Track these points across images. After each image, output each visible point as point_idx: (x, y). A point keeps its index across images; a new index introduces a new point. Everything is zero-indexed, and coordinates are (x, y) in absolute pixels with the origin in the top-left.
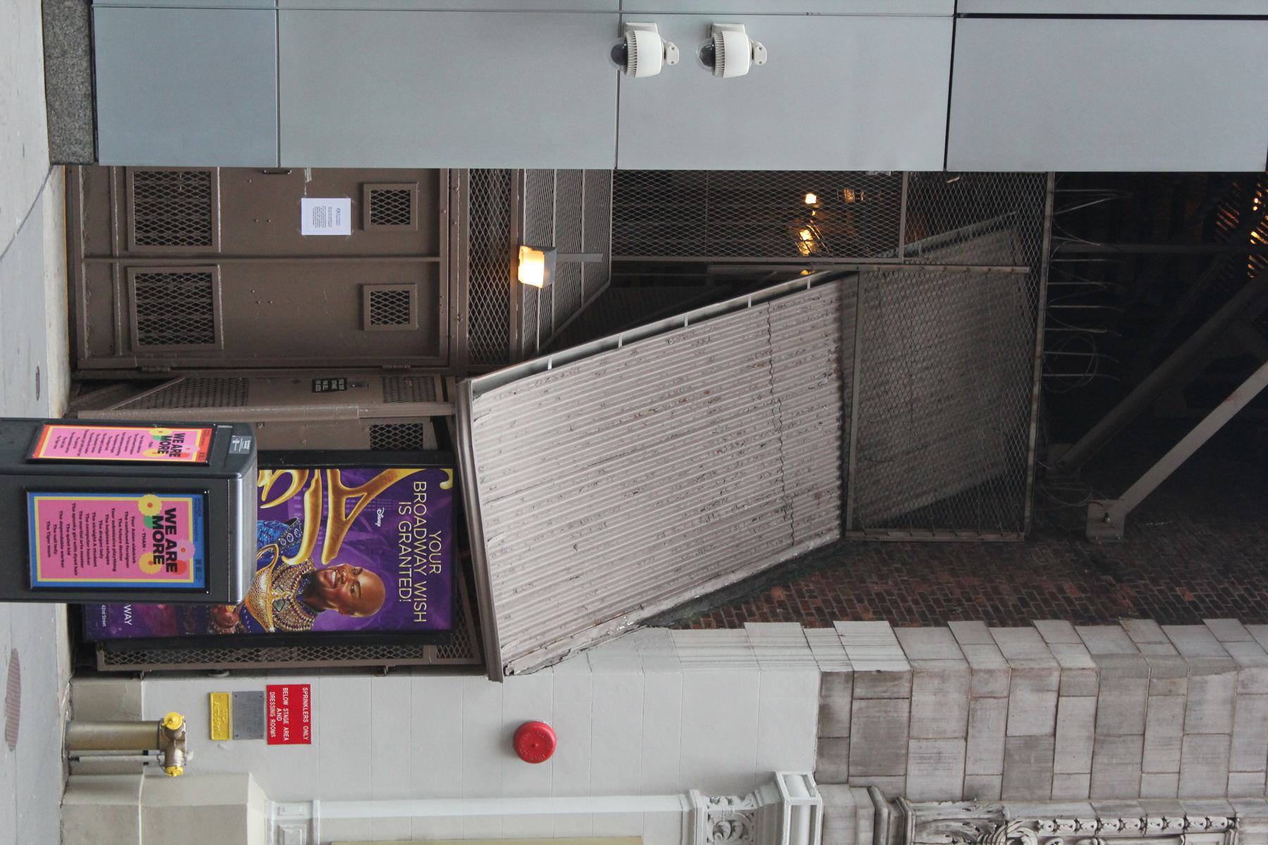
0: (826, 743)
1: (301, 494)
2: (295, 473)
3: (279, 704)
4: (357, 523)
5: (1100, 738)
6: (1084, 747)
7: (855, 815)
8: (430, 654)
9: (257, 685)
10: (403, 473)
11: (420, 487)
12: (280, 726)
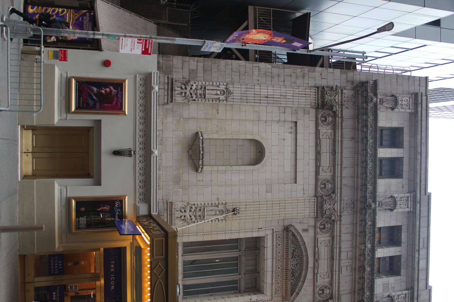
0: (159, 68)
1: (66, 13)
2: (65, 9)
3: (62, 53)
4: (76, 20)
5: (205, 71)
6: (202, 72)
7: (164, 76)
8: (89, 46)
9: (58, 49)
10: (85, 11)
11: (88, 14)
12: (62, 57)
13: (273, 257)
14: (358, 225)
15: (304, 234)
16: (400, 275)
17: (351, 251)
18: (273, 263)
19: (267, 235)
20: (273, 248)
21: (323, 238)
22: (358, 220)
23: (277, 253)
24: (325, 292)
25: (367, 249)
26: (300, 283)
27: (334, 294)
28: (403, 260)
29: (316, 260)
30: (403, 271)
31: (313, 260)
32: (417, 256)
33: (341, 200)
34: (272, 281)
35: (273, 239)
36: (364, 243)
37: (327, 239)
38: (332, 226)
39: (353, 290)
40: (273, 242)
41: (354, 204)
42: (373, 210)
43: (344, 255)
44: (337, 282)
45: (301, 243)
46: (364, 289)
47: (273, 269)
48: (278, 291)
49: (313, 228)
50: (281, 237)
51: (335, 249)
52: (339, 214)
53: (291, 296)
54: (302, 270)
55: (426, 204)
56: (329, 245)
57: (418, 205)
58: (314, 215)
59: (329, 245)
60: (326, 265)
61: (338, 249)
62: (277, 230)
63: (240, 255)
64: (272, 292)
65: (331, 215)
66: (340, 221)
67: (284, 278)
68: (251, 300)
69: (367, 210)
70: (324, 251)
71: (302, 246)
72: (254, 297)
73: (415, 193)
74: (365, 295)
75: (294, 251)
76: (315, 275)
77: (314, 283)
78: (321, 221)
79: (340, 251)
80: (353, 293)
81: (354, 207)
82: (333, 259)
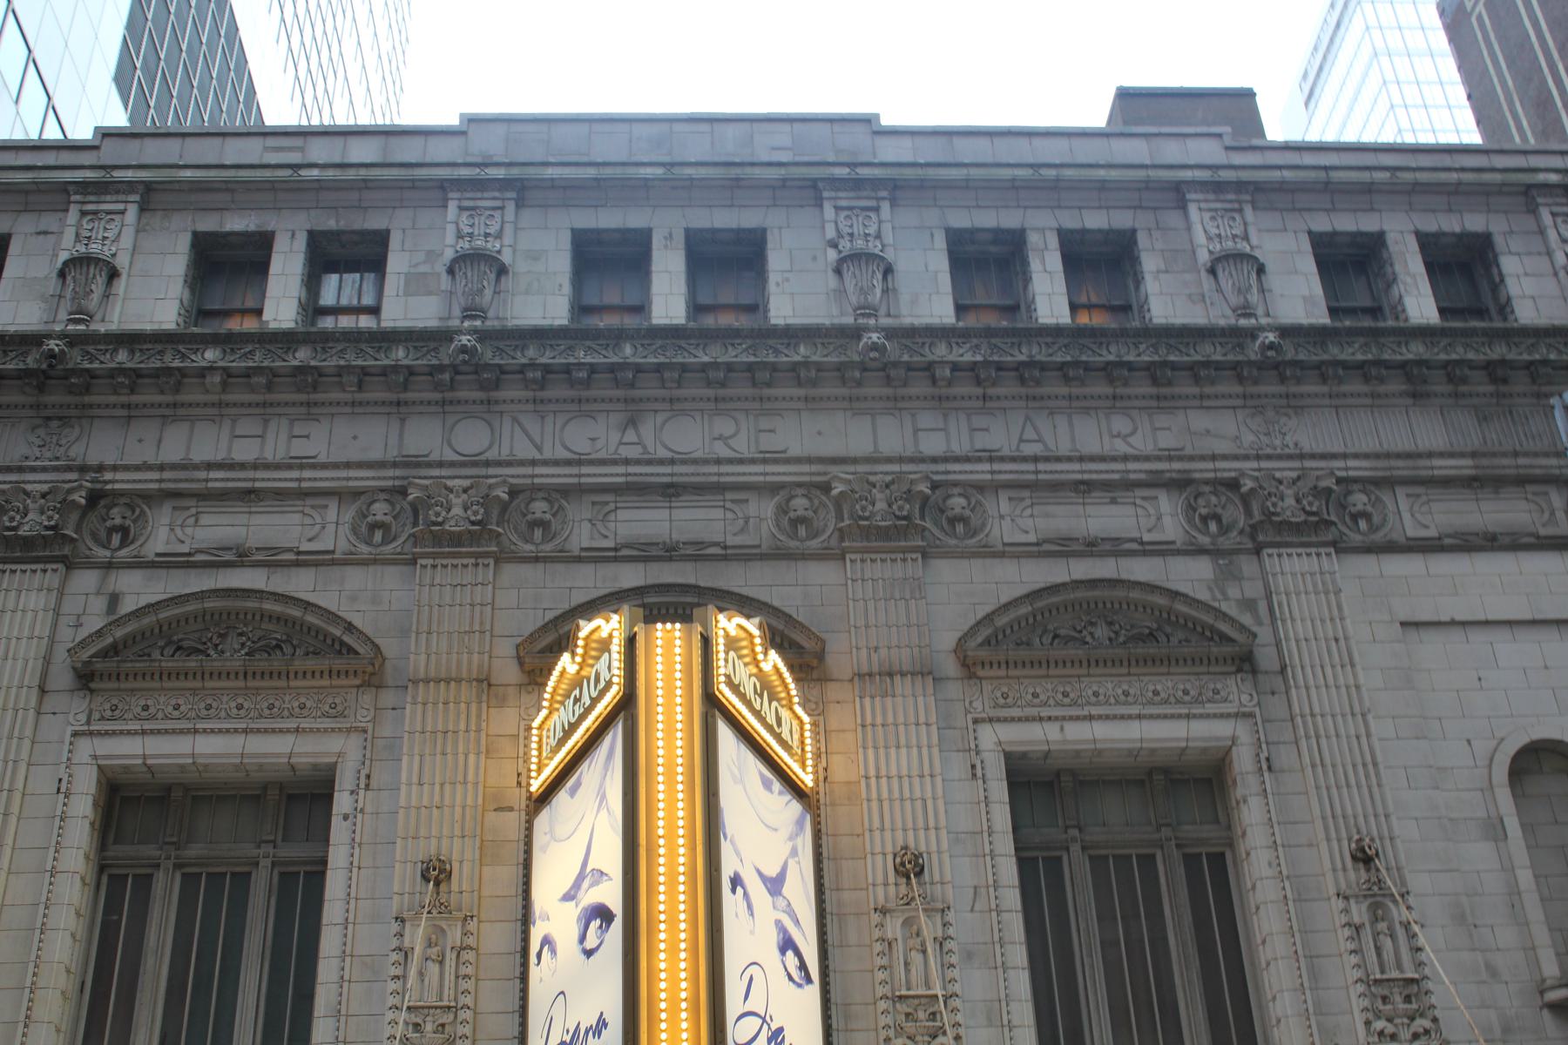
13: (188, 731)
14: (135, 399)
15: (128, 606)
16: (388, 232)
17: (234, 421)
18: (212, 731)
19: (95, 757)
20: (152, 732)
21: (161, 534)
22: (112, 399)
23: (176, 713)
24: (379, 517)
25: (221, 364)
26: (311, 618)
27: (390, 483)
28: (331, 224)
29: (242, 557)
30: (374, 222)
31: (238, 571)
32: (315, 172)
33: (20, 469)
34: (289, 731)
35: (114, 733)
36: (202, 373)
37: (166, 520)
38: (123, 500)
39: (394, 410)
40: (129, 733)
41: (49, 418)
42: (71, 344)
43: (245, 451)
44: (343, 473)
45: (147, 621)
46: (385, 367)
47: (236, 731)
48: (334, 706)
49: (113, 574)
50: (115, 701)
51: (210, 485)
52: (74, 476)
53: (357, 653)
54: (264, 616)
55: (136, 143)
56: (193, 511)
57: (118, 174)
58: (55, 571)
59: (193, 511)
60: (276, 519)
61: (213, 475)
62: (83, 718)
63: (177, 866)
64: (333, 730)
65: (66, 506)
66: (101, 468)
67: (283, 683)
68: (346, 817)
69: (70, 366)
70: (219, 528)
71: (161, 616)
72: (342, 802)
73: (71, 188)
74: (406, 362)
75: (179, 648)
76: (302, 560)
77: (334, 563)
78: (90, 544)
79: (220, 466)
80: (403, 409)
81: (60, 418)
82: (250, 491)
